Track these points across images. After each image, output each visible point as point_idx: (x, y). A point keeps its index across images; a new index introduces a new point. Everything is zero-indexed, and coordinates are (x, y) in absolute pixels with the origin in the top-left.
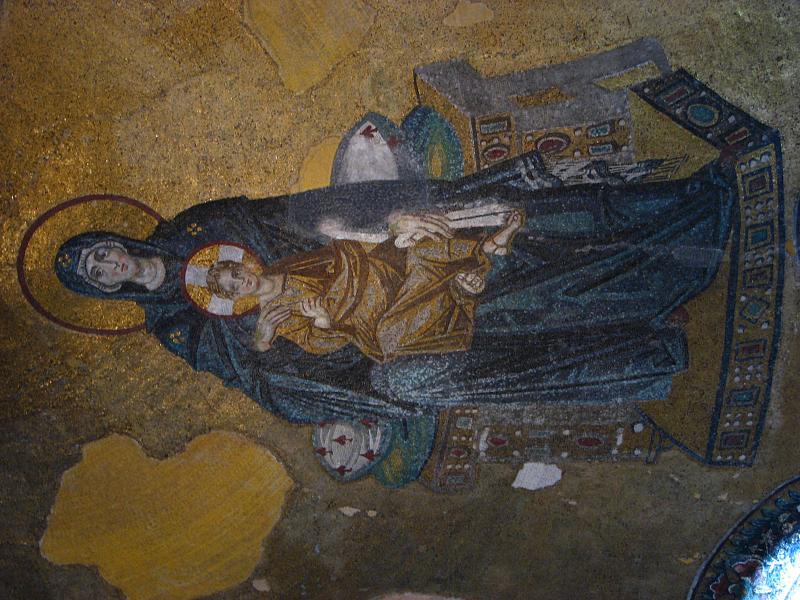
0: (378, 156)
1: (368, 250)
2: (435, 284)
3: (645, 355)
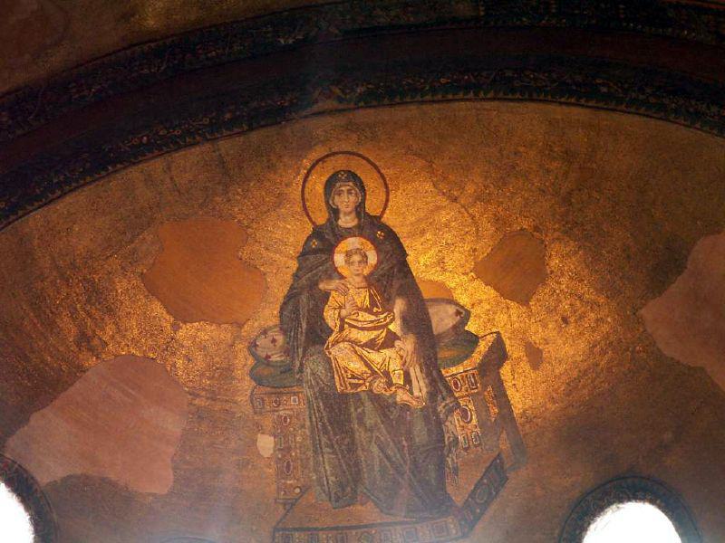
1: (391, 327)
3: (342, 486)
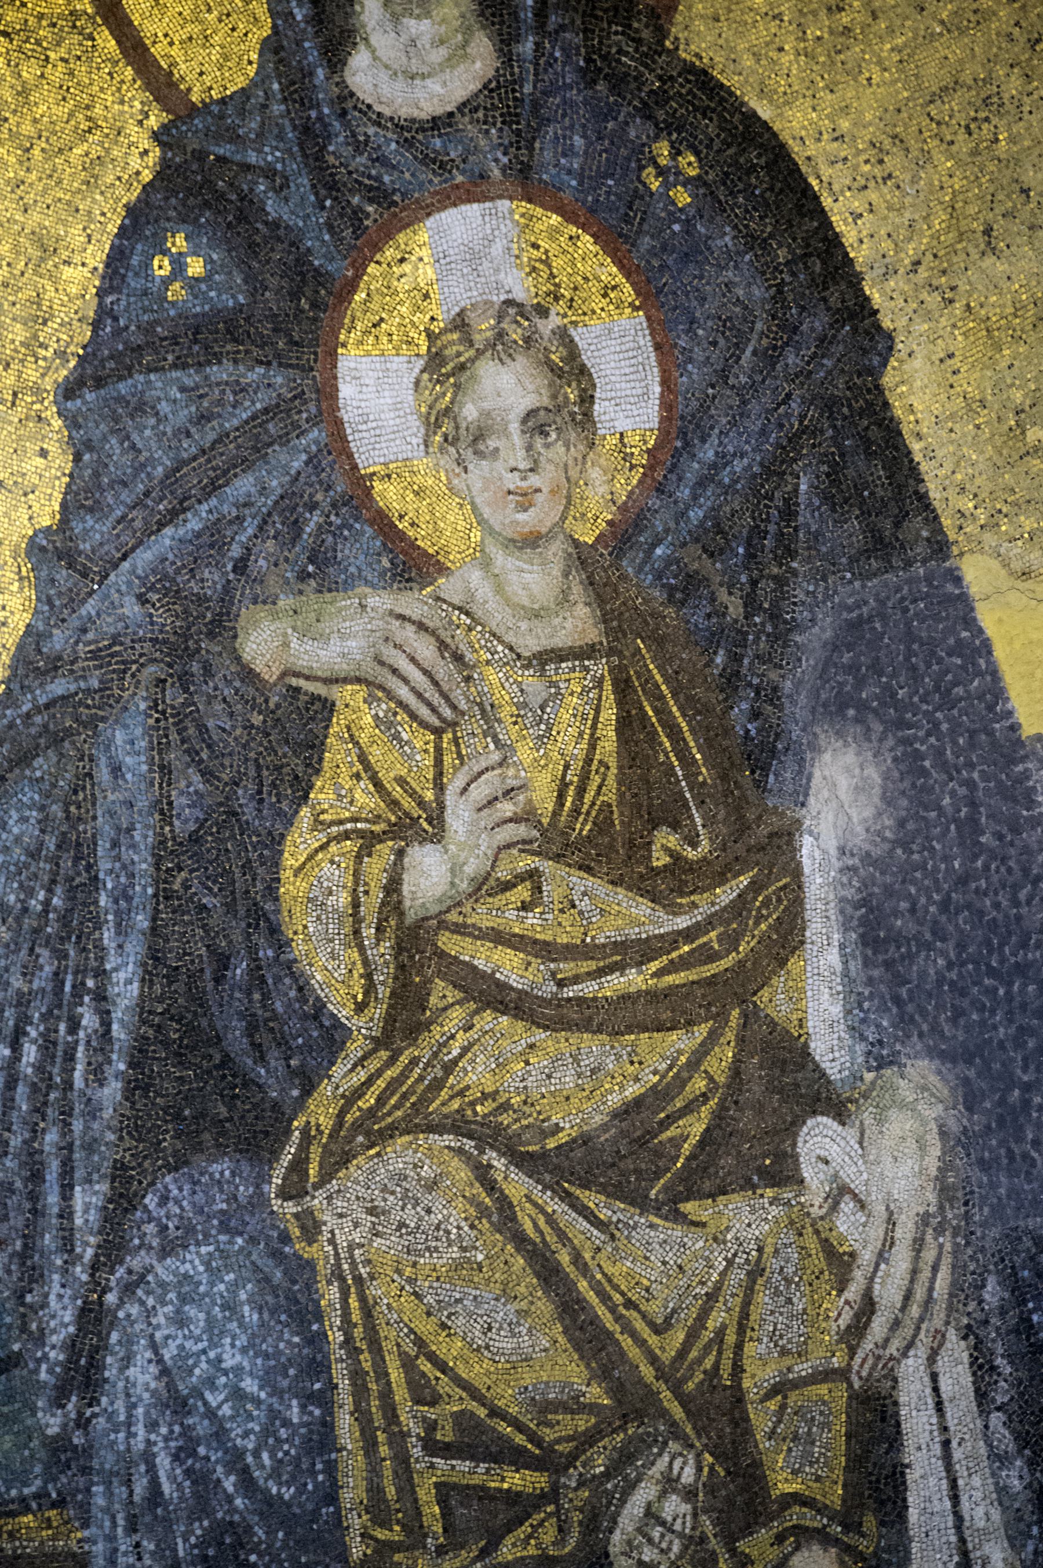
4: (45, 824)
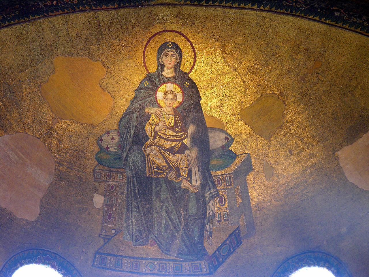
0: (218, 142)
1: (185, 141)
2: (172, 164)
3: (140, 232)
4: (128, 120)
